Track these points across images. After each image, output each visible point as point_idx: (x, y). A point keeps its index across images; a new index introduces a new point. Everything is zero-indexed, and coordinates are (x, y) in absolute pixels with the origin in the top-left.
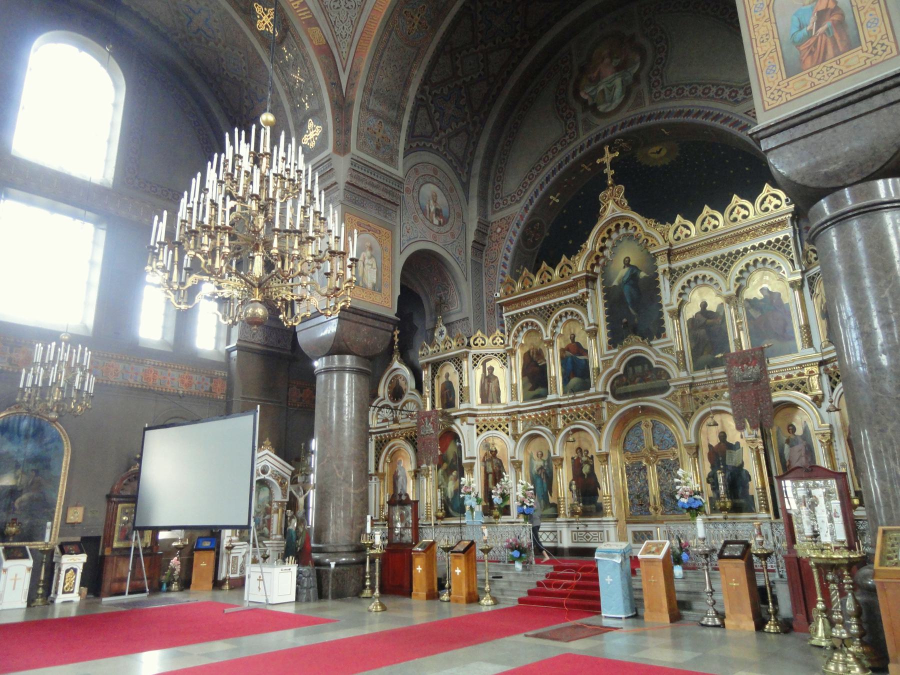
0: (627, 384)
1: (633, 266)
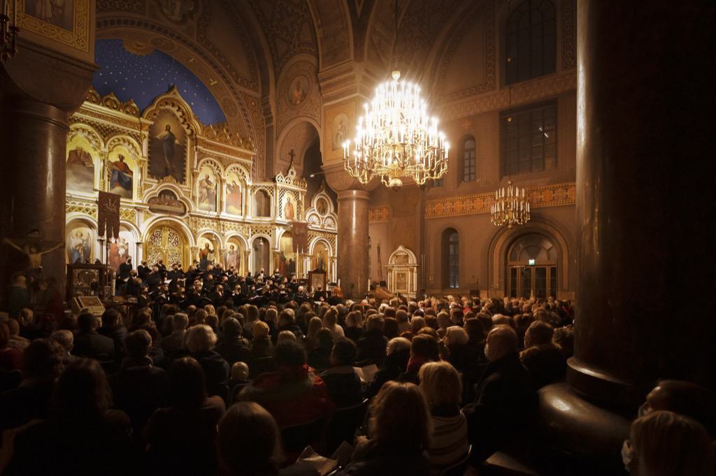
0: (159, 204)
1: (170, 132)
